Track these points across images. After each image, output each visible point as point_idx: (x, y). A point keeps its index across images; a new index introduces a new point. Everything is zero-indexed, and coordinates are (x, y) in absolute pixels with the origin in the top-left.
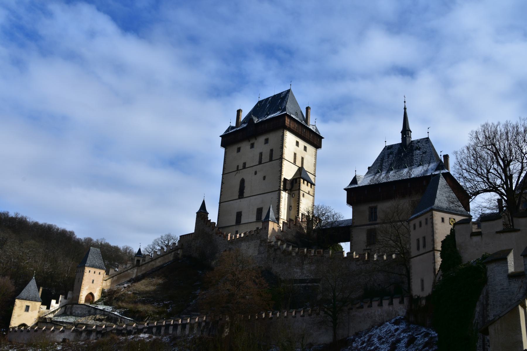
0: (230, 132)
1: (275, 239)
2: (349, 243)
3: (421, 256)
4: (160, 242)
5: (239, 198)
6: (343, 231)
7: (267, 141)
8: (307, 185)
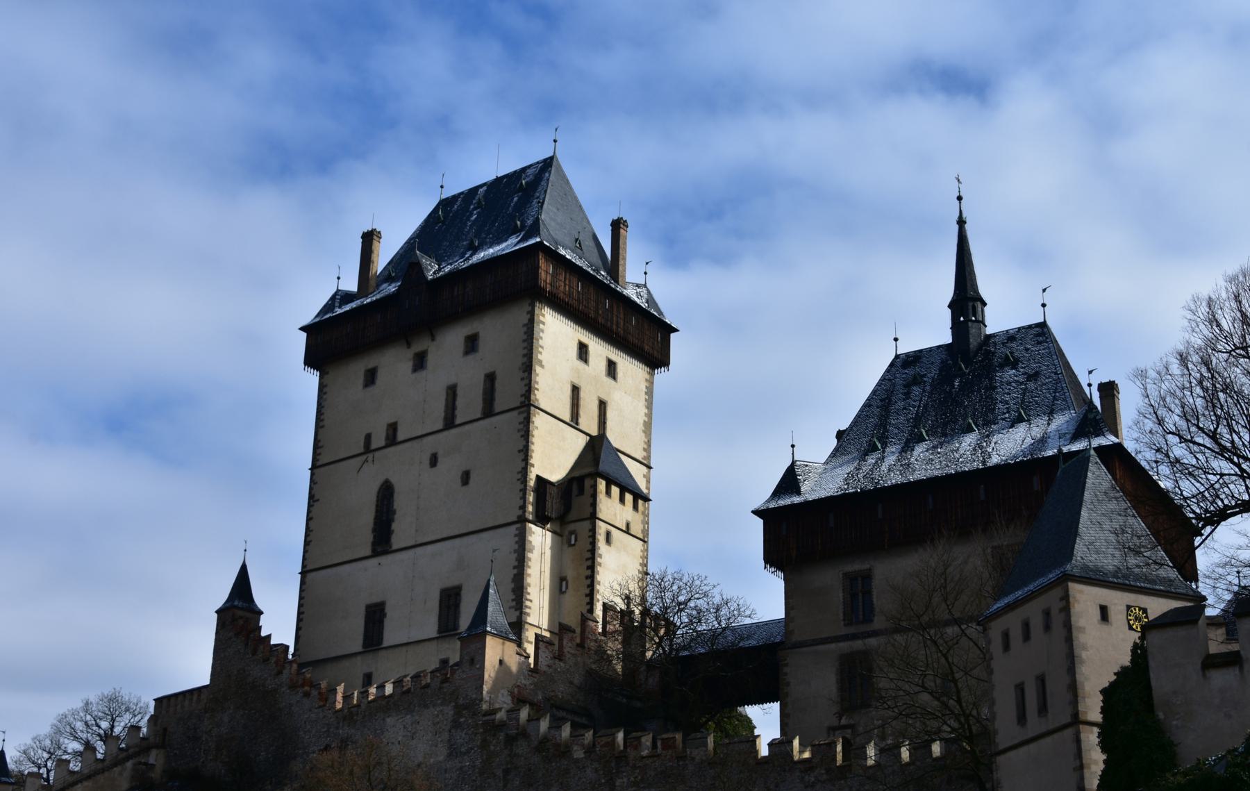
0: (339, 311)
1: (508, 699)
2: (775, 707)
3: (1032, 746)
4: (79, 725)
5: (376, 553)
6: (751, 663)
7: (472, 344)
8: (622, 500)
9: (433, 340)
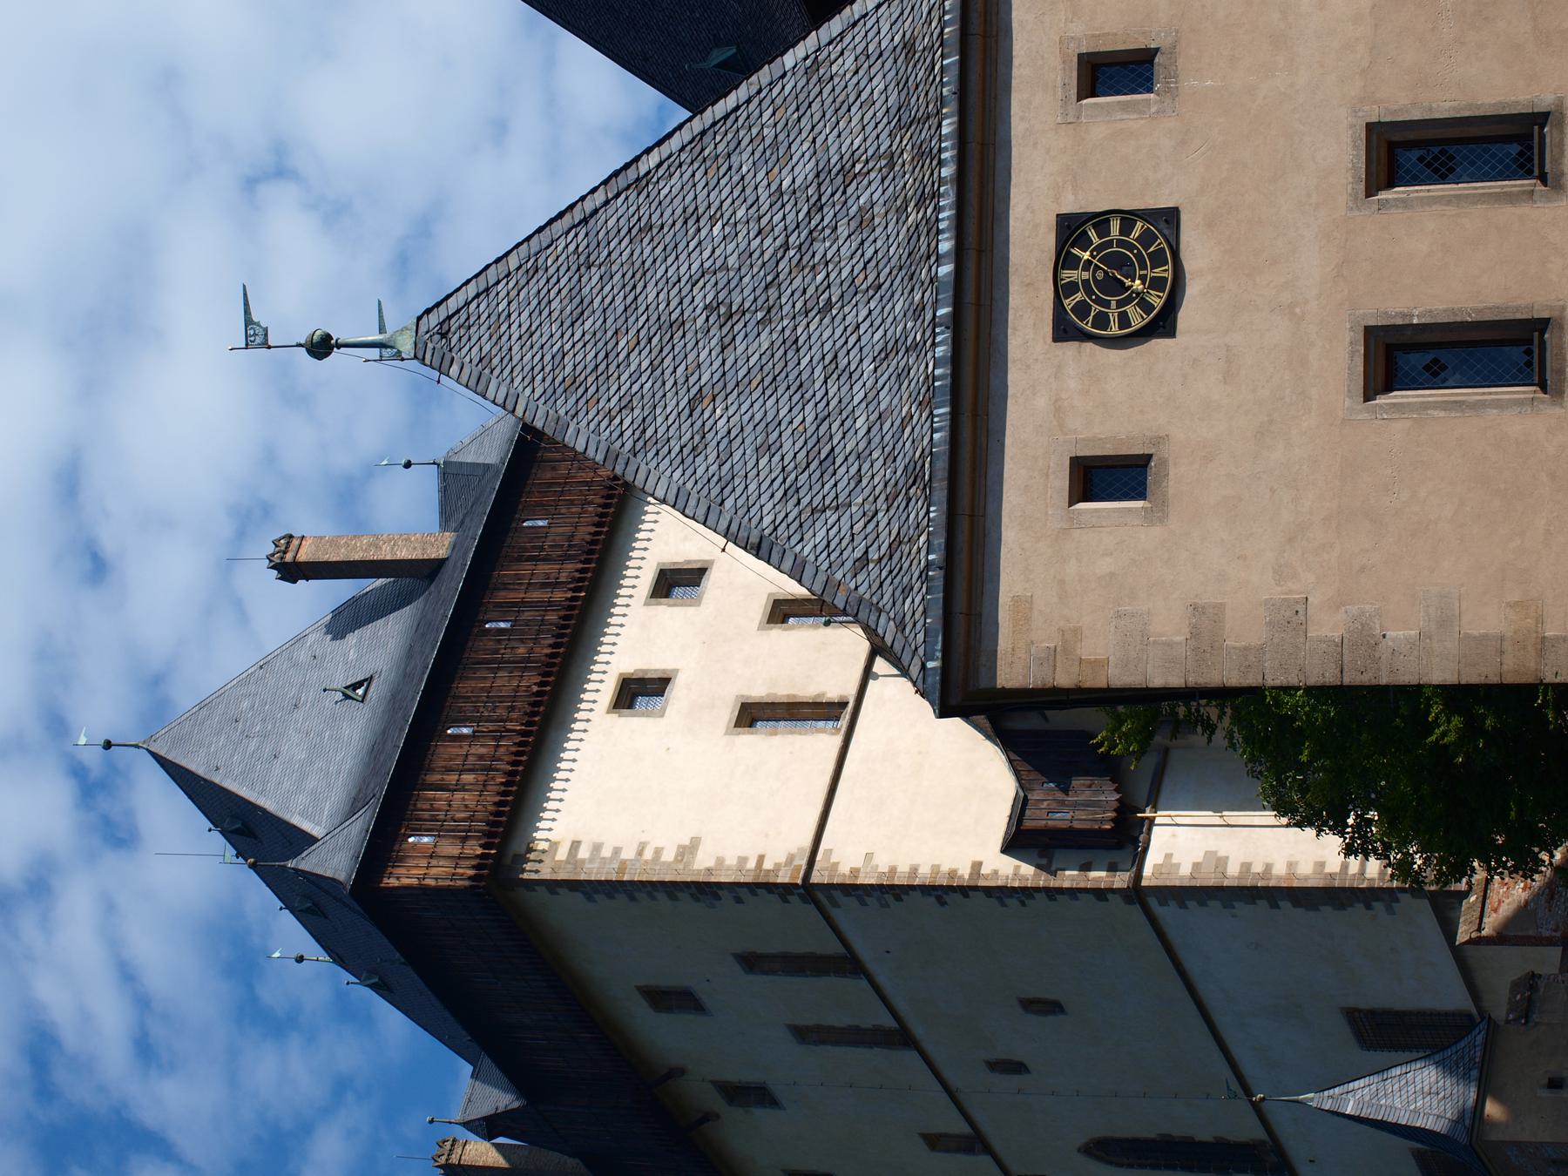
9: (682, 1072)
